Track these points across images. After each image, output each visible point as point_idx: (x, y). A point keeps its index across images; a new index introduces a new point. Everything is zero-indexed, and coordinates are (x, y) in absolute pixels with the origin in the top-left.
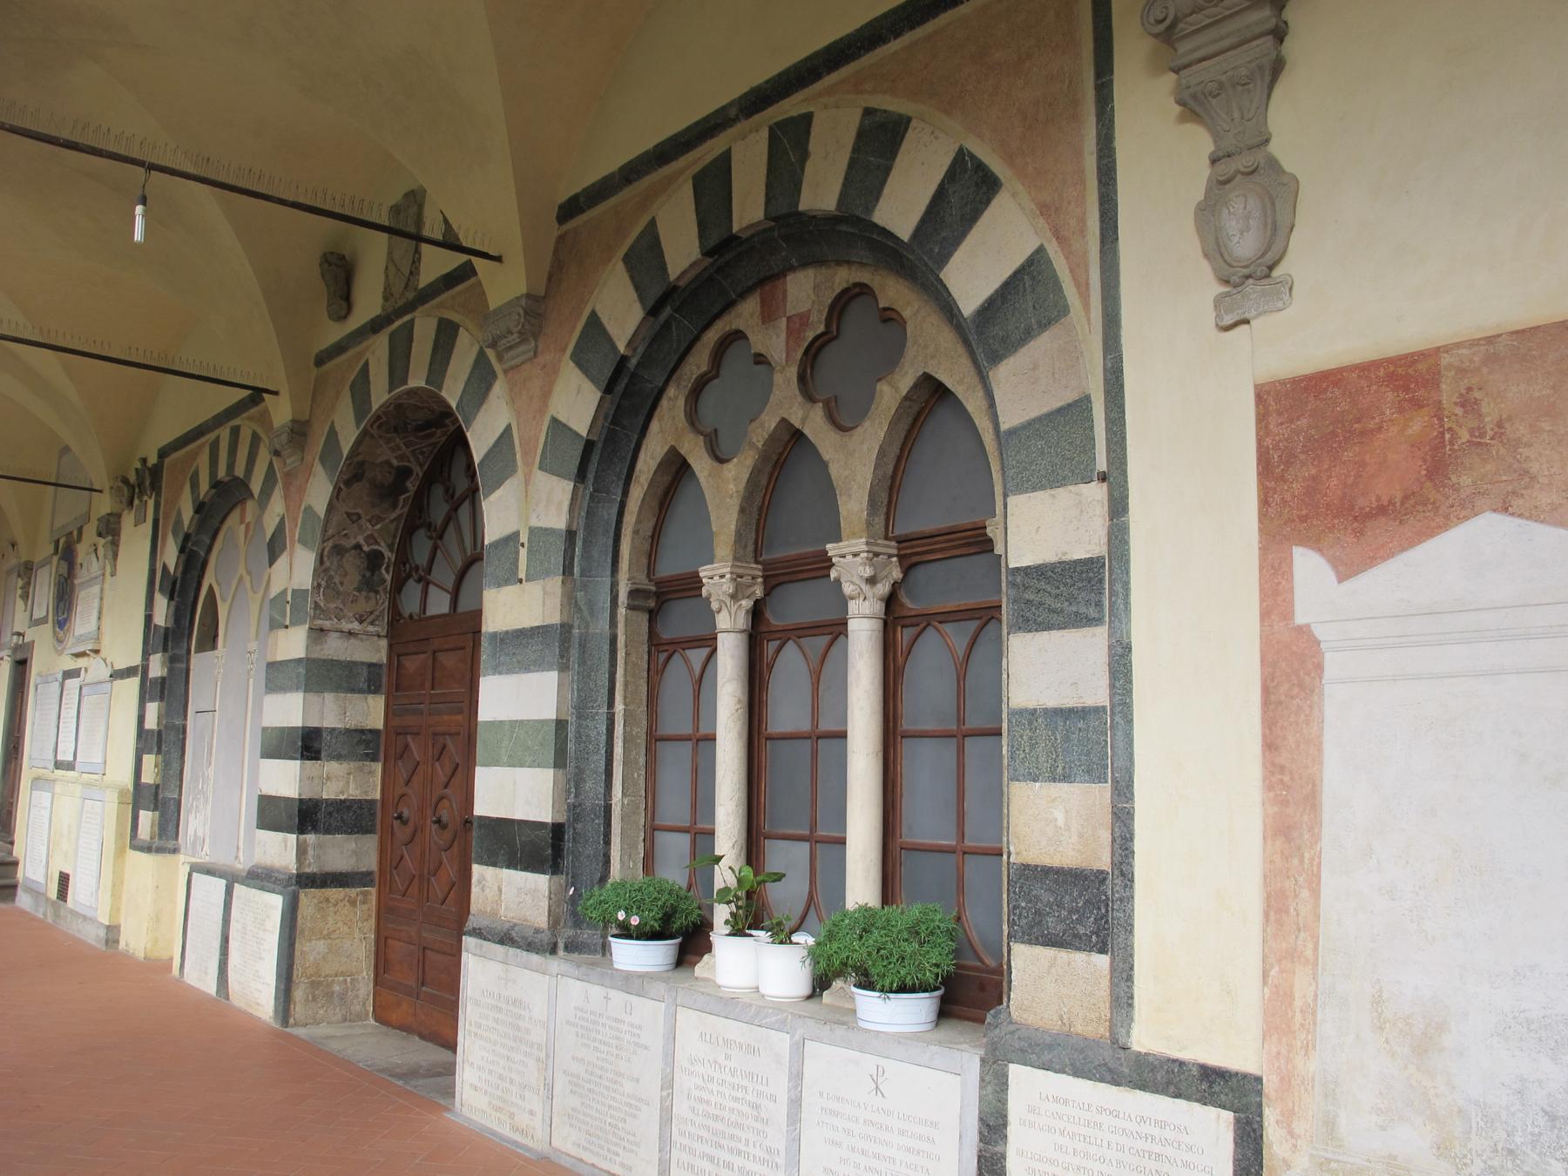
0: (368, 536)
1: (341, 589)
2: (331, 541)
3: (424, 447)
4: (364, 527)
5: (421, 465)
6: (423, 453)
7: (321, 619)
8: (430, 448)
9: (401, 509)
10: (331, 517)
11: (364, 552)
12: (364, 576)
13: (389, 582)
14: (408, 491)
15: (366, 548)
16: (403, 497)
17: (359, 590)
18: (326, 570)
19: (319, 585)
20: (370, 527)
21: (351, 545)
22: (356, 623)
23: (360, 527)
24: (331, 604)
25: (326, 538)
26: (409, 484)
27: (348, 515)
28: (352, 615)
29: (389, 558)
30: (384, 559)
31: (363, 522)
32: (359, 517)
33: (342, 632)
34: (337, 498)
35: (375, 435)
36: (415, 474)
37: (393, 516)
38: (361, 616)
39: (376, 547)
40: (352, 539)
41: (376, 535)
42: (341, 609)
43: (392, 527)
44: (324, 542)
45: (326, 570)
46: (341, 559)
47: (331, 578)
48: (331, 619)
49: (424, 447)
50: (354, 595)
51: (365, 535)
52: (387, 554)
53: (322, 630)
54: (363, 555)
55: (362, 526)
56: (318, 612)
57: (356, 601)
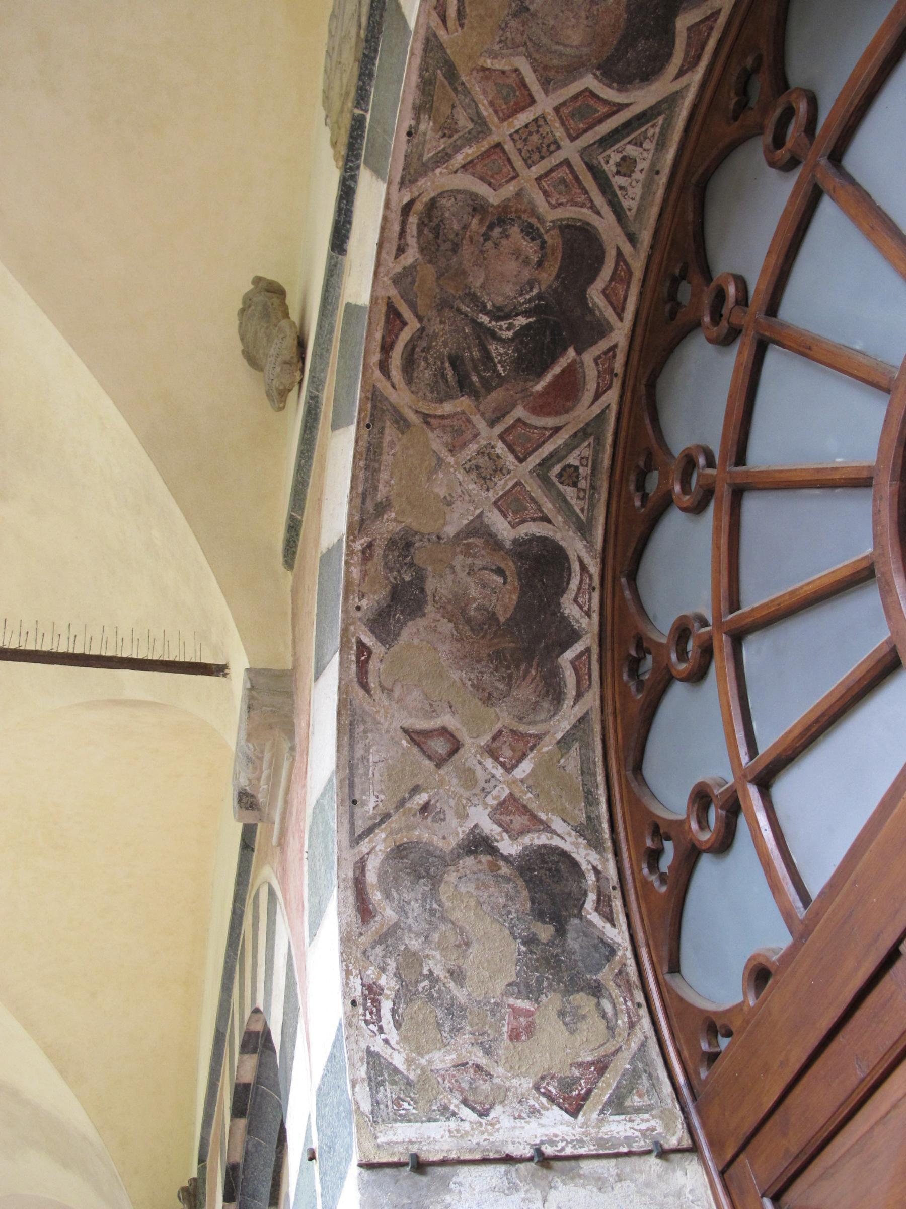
0: (502, 804)
1: (460, 995)
2: (380, 835)
3: (569, 447)
4: (480, 773)
5: (584, 529)
6: (570, 475)
7: (406, 1119)
8: (584, 450)
9: (579, 696)
10: (359, 752)
11: (506, 859)
12: (530, 941)
13: (625, 952)
14: (574, 636)
15: (508, 847)
16: (570, 654)
17: (532, 991)
18: (388, 937)
19: (372, 992)
20: (499, 772)
21: (453, 842)
22: (556, 1113)
23: (468, 777)
24: (437, 1055)
25: (361, 826)
26: (570, 608)
27: (417, 737)
28: (527, 1084)
29: (595, 869)
30: (581, 875)
31: (469, 755)
32: (456, 747)
33: (508, 1159)
34: (365, 686)
35: (412, 417)
36: (576, 567)
37: (563, 724)
38: (567, 1085)
39: (543, 839)
40: (452, 820)
41: (527, 798)
42: (478, 1068)
43: (572, 762)
44: (356, 840)
45: (388, 937)
46: (434, 889)
47: (412, 960)
48: (447, 1112)
49: (569, 447)
50: (516, 1012)
51: (491, 801)
52: (585, 857)
53: (419, 1166)
54: (505, 870)
55: (471, 771)
56: (387, 1093)
57: (530, 1029)
